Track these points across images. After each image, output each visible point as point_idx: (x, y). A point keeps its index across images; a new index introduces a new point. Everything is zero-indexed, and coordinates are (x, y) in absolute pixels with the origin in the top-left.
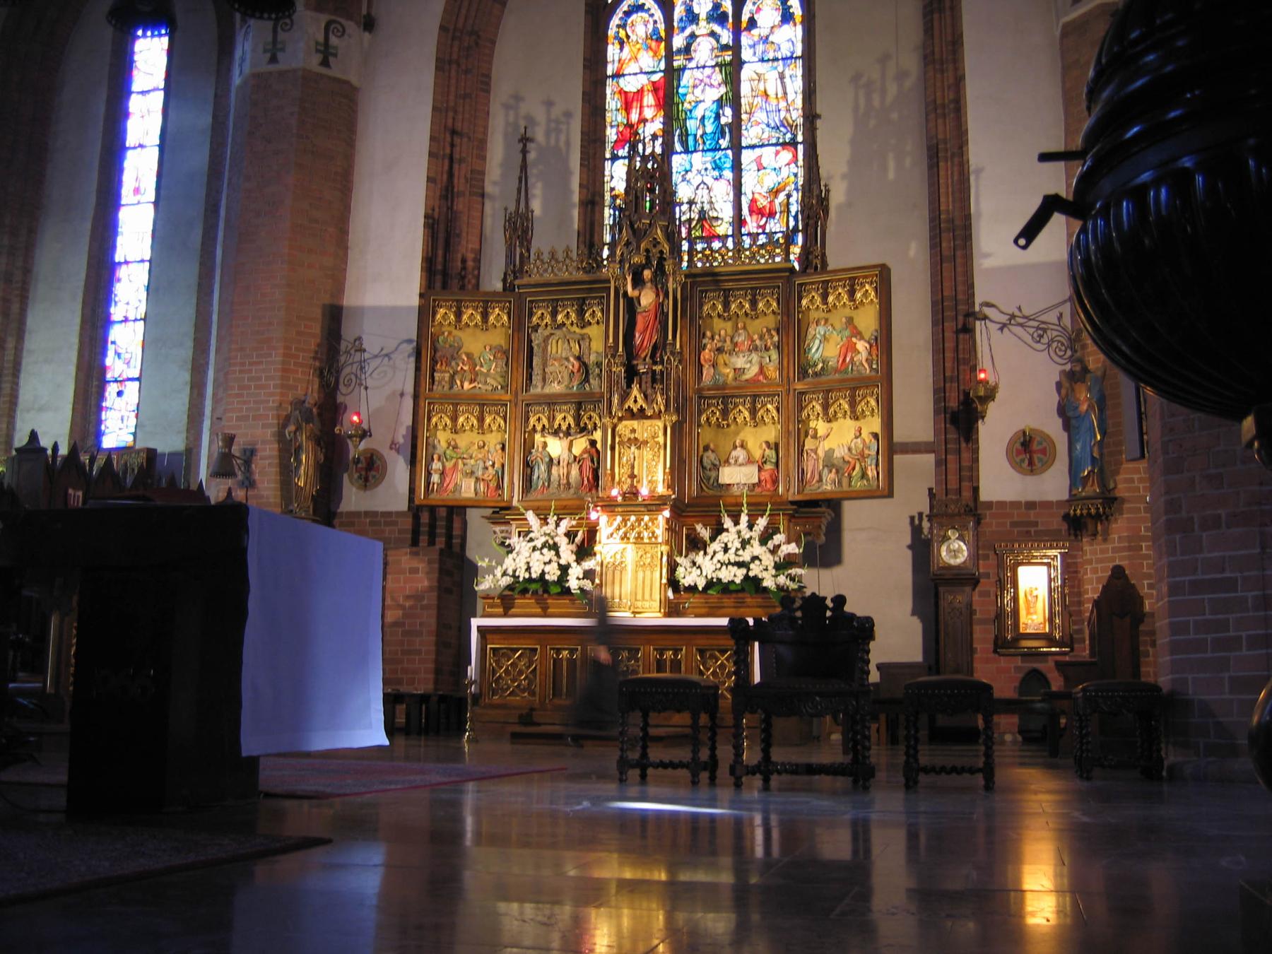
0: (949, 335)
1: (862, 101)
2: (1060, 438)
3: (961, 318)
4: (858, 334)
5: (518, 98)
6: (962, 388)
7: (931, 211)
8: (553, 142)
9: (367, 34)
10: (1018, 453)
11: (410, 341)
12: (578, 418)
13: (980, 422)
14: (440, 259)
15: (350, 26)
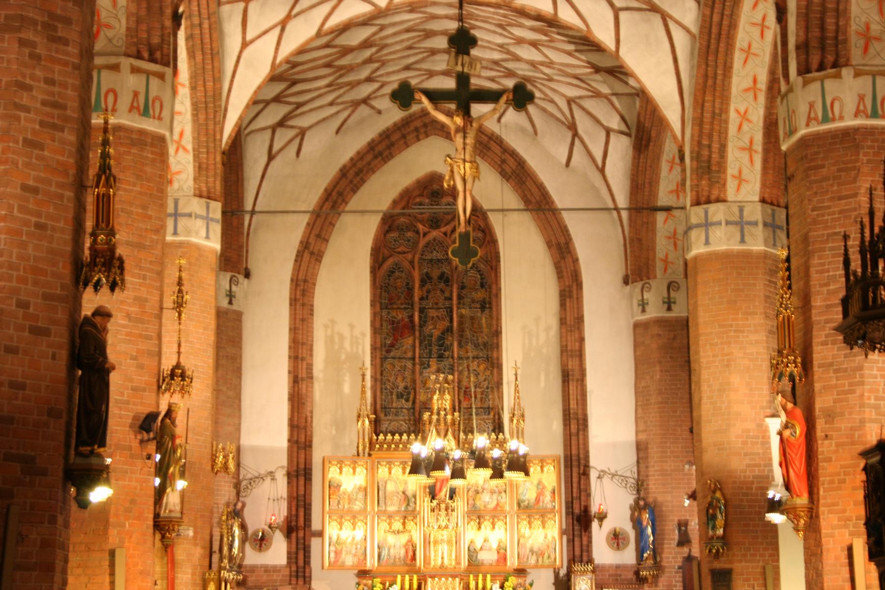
0: (575, 475)
1: (527, 341)
2: (632, 534)
3: (582, 468)
4: (544, 487)
5: (333, 322)
6: (583, 504)
7: (564, 405)
8: (355, 349)
9: (246, 280)
10: (612, 539)
11: (283, 467)
12: (404, 524)
13: (595, 524)
14: (296, 419)
15: (241, 278)
